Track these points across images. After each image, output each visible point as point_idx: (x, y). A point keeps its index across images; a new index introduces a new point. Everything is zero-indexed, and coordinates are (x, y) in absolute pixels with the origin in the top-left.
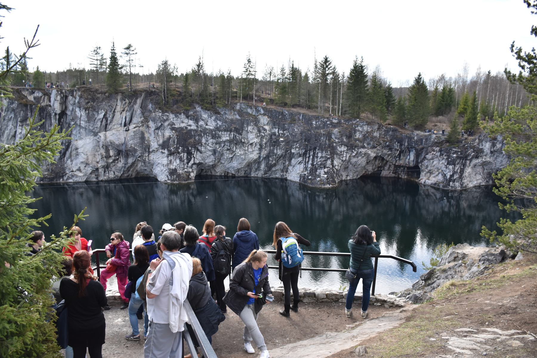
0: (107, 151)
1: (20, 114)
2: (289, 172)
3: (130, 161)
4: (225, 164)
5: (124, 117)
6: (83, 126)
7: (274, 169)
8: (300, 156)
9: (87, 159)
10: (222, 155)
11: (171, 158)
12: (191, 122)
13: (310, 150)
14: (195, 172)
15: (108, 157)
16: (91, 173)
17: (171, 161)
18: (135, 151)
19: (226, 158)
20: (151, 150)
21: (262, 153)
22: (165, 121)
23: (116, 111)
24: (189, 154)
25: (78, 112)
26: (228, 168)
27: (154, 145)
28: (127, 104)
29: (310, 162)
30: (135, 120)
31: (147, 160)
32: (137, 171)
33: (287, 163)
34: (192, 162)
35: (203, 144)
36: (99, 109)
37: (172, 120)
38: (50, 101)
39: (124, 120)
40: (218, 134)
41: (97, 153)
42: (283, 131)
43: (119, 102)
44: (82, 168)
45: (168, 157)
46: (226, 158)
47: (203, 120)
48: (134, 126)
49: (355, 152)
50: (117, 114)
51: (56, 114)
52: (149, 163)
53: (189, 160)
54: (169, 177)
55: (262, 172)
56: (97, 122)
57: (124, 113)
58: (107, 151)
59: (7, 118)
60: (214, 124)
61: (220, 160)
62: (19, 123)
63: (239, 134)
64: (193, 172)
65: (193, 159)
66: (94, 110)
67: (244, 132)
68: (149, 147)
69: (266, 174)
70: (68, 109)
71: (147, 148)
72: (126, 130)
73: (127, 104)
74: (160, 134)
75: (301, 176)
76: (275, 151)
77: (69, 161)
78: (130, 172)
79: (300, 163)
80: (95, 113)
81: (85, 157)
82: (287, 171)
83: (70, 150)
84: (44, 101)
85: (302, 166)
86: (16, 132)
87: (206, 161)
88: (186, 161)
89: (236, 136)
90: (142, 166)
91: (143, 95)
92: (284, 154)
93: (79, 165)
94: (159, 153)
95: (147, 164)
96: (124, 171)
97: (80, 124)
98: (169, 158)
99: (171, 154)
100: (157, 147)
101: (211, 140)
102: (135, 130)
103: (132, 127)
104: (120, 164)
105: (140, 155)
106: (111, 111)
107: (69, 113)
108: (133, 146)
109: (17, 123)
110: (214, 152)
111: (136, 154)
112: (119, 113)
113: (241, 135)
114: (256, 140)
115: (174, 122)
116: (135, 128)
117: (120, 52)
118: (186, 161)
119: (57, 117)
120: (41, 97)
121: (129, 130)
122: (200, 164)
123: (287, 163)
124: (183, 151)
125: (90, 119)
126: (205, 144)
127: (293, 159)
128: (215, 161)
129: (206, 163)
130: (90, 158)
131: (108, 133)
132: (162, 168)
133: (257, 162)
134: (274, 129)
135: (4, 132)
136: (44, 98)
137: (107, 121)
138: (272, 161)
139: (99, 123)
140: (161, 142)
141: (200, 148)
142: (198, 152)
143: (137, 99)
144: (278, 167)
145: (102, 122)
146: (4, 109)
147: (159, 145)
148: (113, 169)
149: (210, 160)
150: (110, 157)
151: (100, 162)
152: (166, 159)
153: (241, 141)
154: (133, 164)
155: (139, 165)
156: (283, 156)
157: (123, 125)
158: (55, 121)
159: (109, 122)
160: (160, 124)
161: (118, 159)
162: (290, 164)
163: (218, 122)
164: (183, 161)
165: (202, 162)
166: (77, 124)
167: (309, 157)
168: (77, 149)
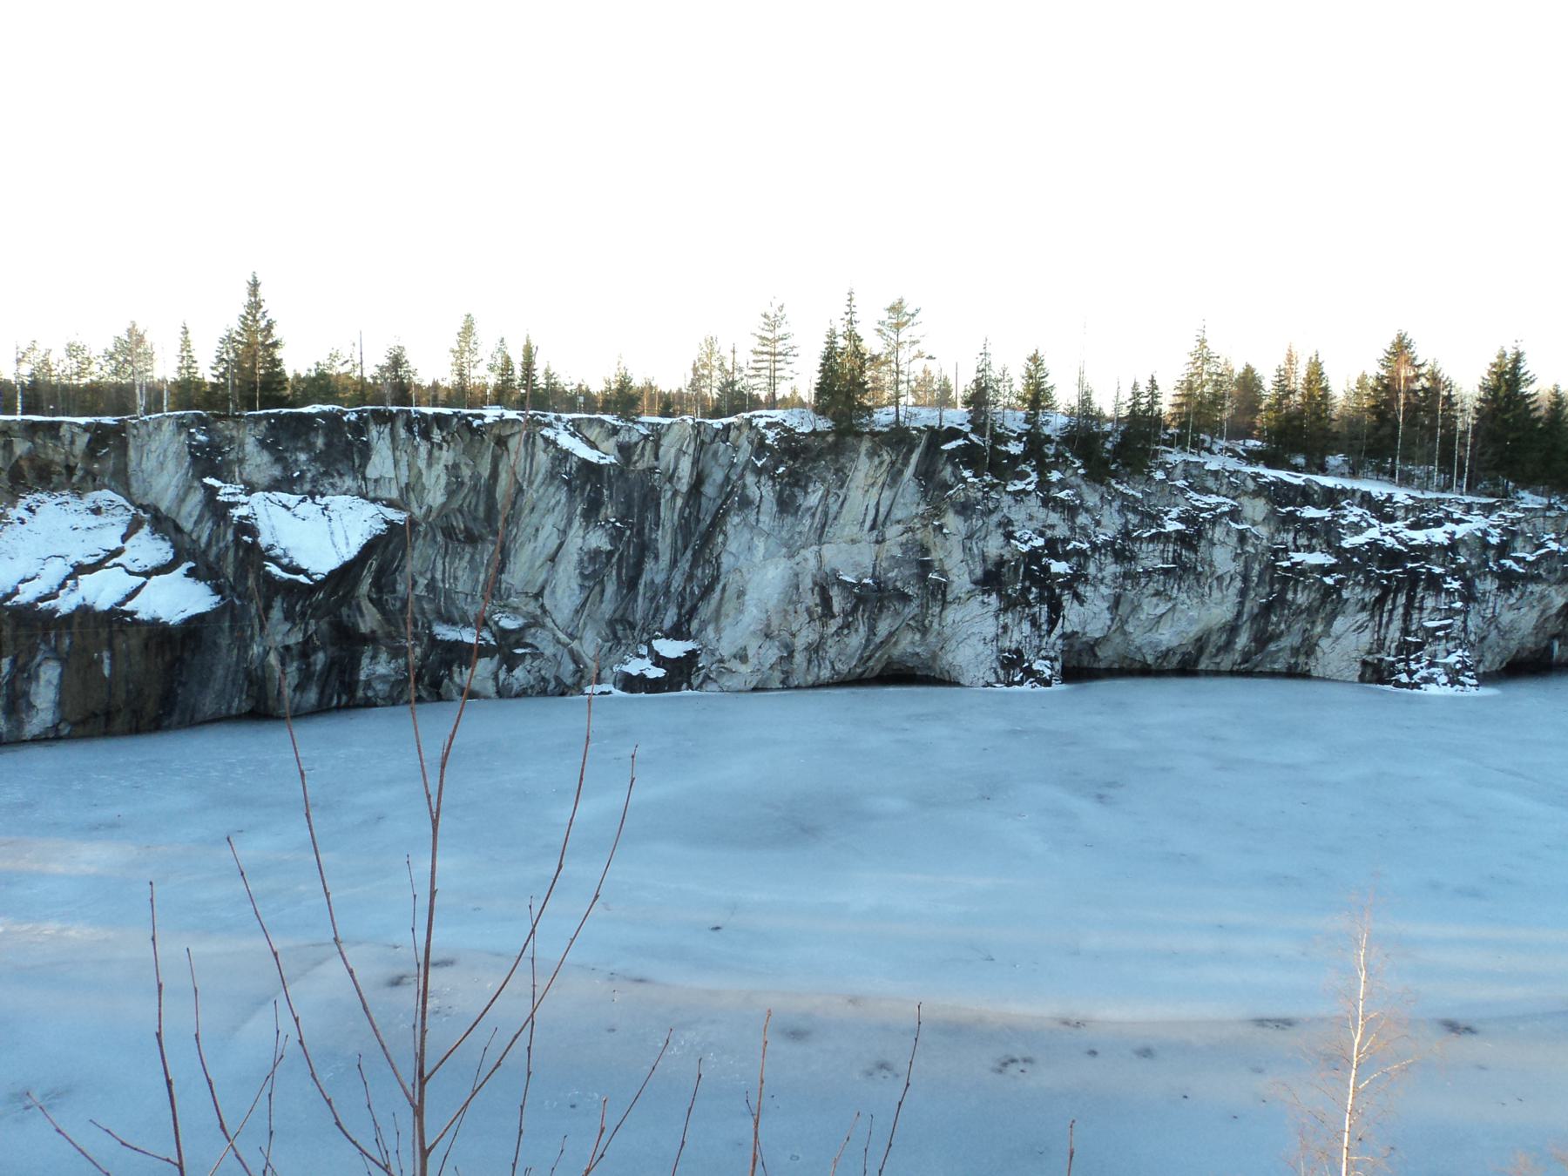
2: (1319, 654)
5: (873, 503)
7: (1272, 647)
8: (1363, 608)
9: (768, 626)
10: (1136, 608)
11: (1008, 618)
12: (1054, 518)
13: (1397, 591)
15: (828, 613)
17: (1005, 628)
18: (905, 598)
19: (1143, 617)
20: (949, 598)
21: (1248, 605)
22: (991, 512)
24: (1056, 609)
25: (753, 492)
26: (1139, 649)
27: (961, 580)
28: (884, 466)
29: (1397, 624)
30: (898, 514)
31: (936, 626)
34: (1057, 631)
38: (657, 458)
39: (872, 513)
40: (1132, 552)
41: (791, 608)
43: (863, 457)
44: (750, 653)
45: (997, 617)
47: (1087, 510)
48: (900, 527)
49: (1517, 594)
51: (675, 493)
53: (1052, 623)
54: (1001, 672)
55: (1237, 657)
57: (875, 491)
58: (826, 601)
59: (542, 505)
61: (1124, 622)
62: (577, 522)
63: (1188, 549)
66: (796, 484)
67: (1203, 543)
71: (938, 593)
72: (877, 542)
73: (884, 466)
75: (1364, 663)
76: (1290, 596)
77: (710, 630)
78: (871, 663)
81: (764, 616)
83: (716, 595)
84: (642, 455)
85: (1366, 638)
86: (560, 546)
88: (1045, 627)
90: (912, 643)
92: (1316, 604)
93: (741, 643)
94: (974, 606)
97: (758, 520)
99: (1008, 605)
104: (856, 640)
105: (917, 611)
107: (709, 490)
108: (899, 584)
112: (861, 491)
113: (1196, 552)
115: (1012, 517)
118: (1045, 627)
119: (679, 502)
120: (637, 444)
121: (884, 540)
123: (1319, 629)
124: (1041, 599)
125: (786, 505)
127: (1340, 618)
130: (775, 622)
131: (828, 551)
132: (981, 647)
133: (1232, 629)
134: (1283, 535)
135: (522, 545)
137: (826, 514)
140: (979, 572)
141: (1081, 589)
145: (813, 515)
147: (975, 583)
148: (832, 653)
150: (833, 616)
151: (804, 632)
152: (991, 621)
154: (891, 634)
156: (1311, 611)
158: (669, 514)
159: (831, 516)
163: (1130, 516)
167: (1391, 612)
168: (741, 594)
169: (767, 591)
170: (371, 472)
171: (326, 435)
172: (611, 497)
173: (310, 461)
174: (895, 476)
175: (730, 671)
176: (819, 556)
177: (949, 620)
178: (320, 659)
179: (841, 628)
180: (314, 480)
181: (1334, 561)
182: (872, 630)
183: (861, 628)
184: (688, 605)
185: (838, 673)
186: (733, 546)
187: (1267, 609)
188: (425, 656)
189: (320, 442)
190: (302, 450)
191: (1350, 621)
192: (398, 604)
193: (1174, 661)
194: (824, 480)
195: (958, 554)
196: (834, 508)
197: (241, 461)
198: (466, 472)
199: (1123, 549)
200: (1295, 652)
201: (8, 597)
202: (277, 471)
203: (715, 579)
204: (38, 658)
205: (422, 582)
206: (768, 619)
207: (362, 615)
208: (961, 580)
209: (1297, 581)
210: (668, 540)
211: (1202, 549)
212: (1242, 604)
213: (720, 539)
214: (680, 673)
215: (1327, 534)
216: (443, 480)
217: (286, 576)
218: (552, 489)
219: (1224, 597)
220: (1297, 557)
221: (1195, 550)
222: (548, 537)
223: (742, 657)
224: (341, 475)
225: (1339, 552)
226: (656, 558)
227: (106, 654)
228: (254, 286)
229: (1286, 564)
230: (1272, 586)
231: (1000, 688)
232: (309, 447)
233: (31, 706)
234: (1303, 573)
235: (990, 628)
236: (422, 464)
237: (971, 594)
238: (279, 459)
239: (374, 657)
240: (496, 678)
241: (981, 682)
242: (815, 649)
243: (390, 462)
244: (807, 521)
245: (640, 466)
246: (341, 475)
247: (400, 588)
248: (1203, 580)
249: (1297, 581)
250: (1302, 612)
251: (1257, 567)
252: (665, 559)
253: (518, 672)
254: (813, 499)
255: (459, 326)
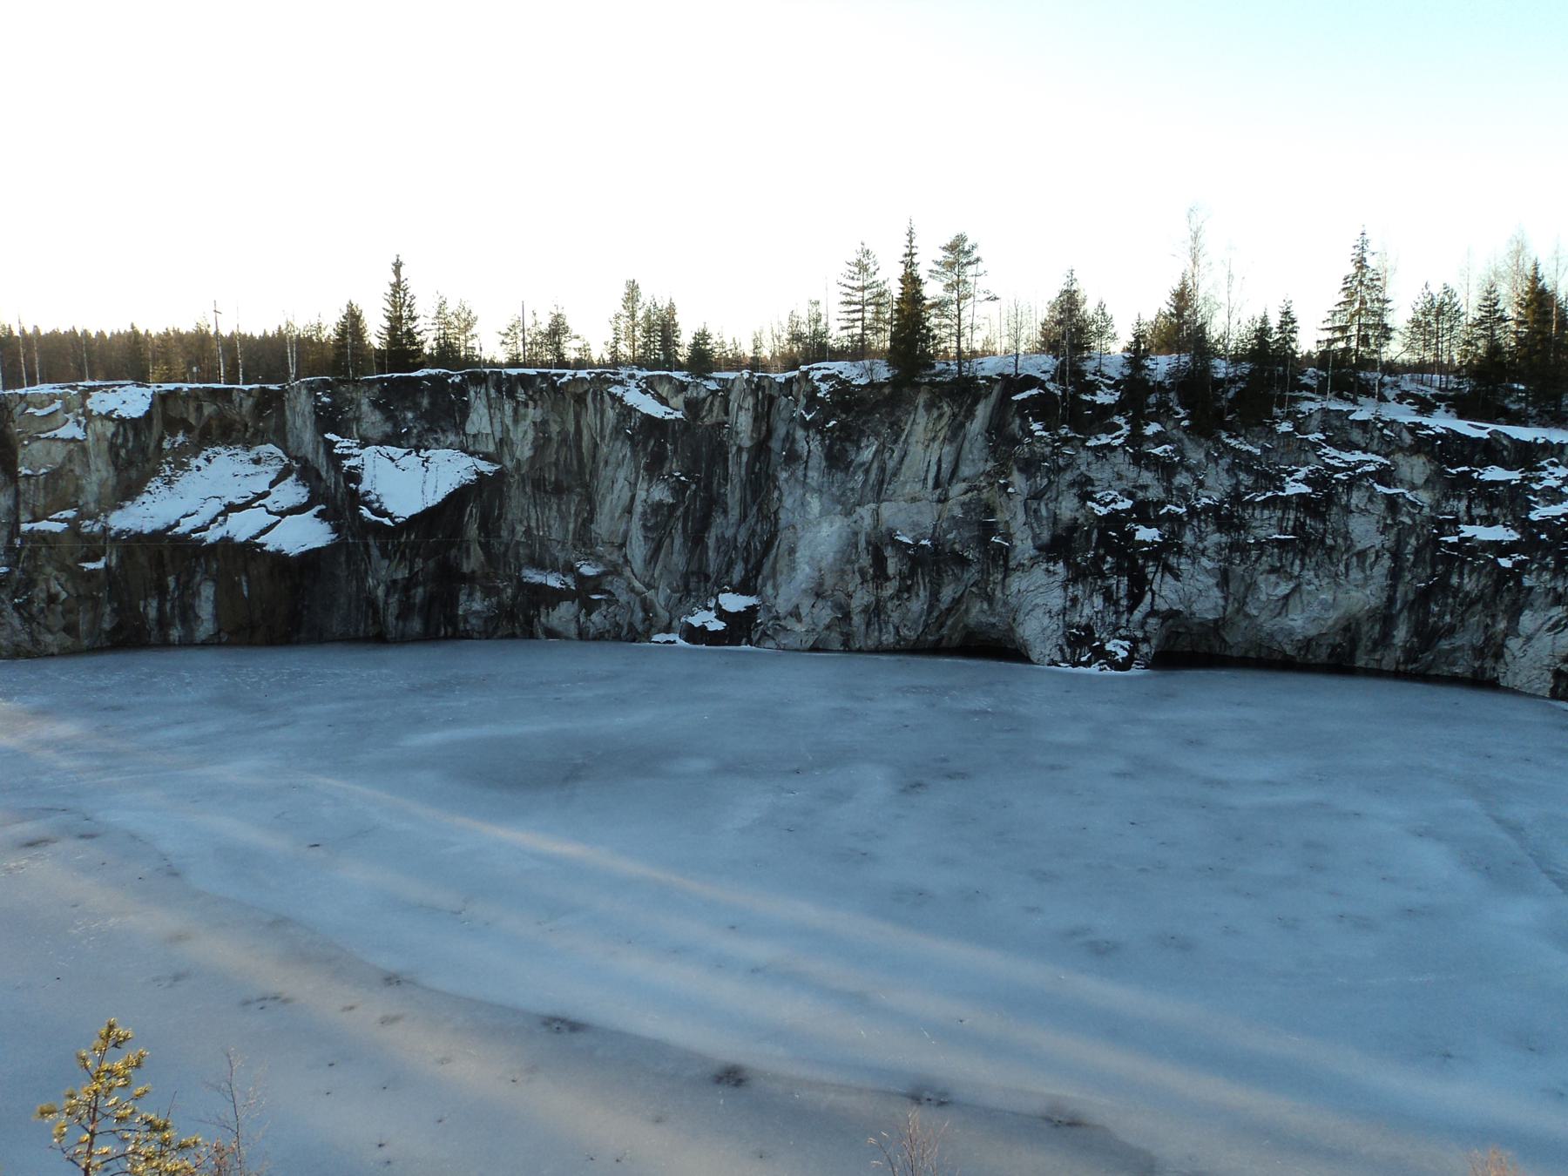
0: (879, 561)
1: (645, 449)
2: (1508, 658)
3: (947, 593)
4: (1262, 619)
5: (934, 460)
6: (814, 484)
7: (1444, 645)
9: (821, 585)
10: (1252, 587)
12: (1147, 477)
14: (1154, 642)
16: (828, 627)
17: (1074, 600)
18: (964, 562)
19: (1263, 597)
20: (1012, 564)
21: (1401, 589)
22: (1060, 470)
23: (912, 440)
25: (802, 447)
27: (1024, 546)
28: (945, 420)
30: (966, 471)
31: (998, 594)
32: (966, 626)
33: (1502, 625)
34: (1144, 607)
35: (1186, 548)
36: (862, 433)
37: (1083, 468)
38: (727, 414)
39: (934, 469)
40: (1241, 518)
42: (1489, 509)
43: (921, 411)
44: (804, 611)
45: (1066, 589)
46: (1263, 597)
47: (1188, 469)
48: (964, 485)
50: (916, 450)
51: (740, 449)
52: (1005, 603)
53: (1135, 599)
54: (1067, 650)
56: (855, 473)
57: (936, 445)
58: (879, 561)
59: (612, 460)
60: (1227, 482)
61: (1243, 603)
64: (1146, 640)
65: (1148, 596)
66: (848, 438)
68: (1004, 554)
69: (1415, 661)
70: (775, 436)
71: (1000, 559)
72: (939, 501)
73: (945, 420)
74: (1044, 512)
76: (1455, 580)
77: (769, 584)
78: (945, 631)
79: (1555, 626)
80: (848, 445)
82: (1498, 656)
84: (711, 410)
86: (633, 498)
87: (1195, 607)
89: (1303, 524)
91: (995, 393)
93: (795, 600)
94: (1038, 575)
95: (999, 608)
96: (926, 625)
97: (805, 476)
98: (1071, 589)
99: (1077, 575)
100: (1033, 552)
101: (1216, 537)
102: (966, 498)
103: (957, 489)
104: (917, 605)
105: (977, 576)
106: (895, 442)
107: (775, 445)
108: (957, 547)
109: (637, 473)
110: (1224, 579)
111: (966, 576)
112: (920, 447)
114: (1378, 540)
115: (1092, 475)
116: (966, 493)
117: (928, 260)
118: (1124, 602)
119: (745, 457)
120: (705, 400)
122: (1172, 614)
123: (1502, 625)
124: (1118, 570)
126: (1193, 548)
128: (1225, 609)
129: (1193, 614)
130: (829, 581)
131: (887, 510)
132: (1046, 621)
133: (1385, 617)
135: (604, 496)
136: (712, 403)
137: (882, 469)
138: (1441, 615)
139: (860, 477)
140: (1046, 536)
141: (1173, 560)
142: (1168, 578)
143: (976, 402)
144: (1461, 639)
145: (867, 472)
146: (608, 432)
147: (1039, 548)
148: (895, 617)
149: (1208, 605)
150: (888, 579)
151: (859, 594)
152: (1059, 592)
153: (1322, 541)
154: (957, 602)
155: (974, 611)
157: (930, 482)
159: (888, 473)
160: (1045, 481)
161: (909, 589)
162: (1512, 630)
163: (1242, 476)
164: (1117, 603)
165: (1181, 608)
166: (797, 480)
169: (822, 549)
170: (471, 429)
171: (431, 396)
172: (675, 452)
173: (416, 419)
174: (956, 431)
175: (784, 629)
176: (876, 513)
177: (1014, 588)
178: (419, 593)
179: (900, 591)
180: (419, 436)
181: (1516, 536)
182: (934, 596)
183: (922, 593)
184: (753, 560)
185: (905, 639)
186: (788, 502)
187: (1425, 596)
188: (515, 597)
189: (425, 402)
190: (409, 409)
191: (1541, 617)
192: (502, 549)
193: (1323, 654)
194: (877, 435)
195: (1021, 517)
196: (891, 464)
197: (358, 420)
198: (554, 428)
199: (1231, 515)
200: (1479, 653)
201: (170, 528)
202: (388, 428)
203: (774, 535)
204: (198, 578)
205: (520, 529)
206: (821, 577)
207: (468, 557)
208: (1024, 546)
209: (1464, 562)
210: (738, 495)
211: (1334, 518)
212: (1393, 587)
213: (776, 494)
214: (739, 628)
215: (1510, 502)
216: (531, 435)
217: (374, 518)
218: (619, 444)
219: (1366, 579)
220: (1468, 531)
221: (1322, 518)
222: (621, 492)
223: (795, 614)
224: (444, 431)
225: (1524, 525)
226: (725, 512)
227: (244, 578)
228: (397, 267)
229: (1453, 539)
230: (1434, 568)
231: (1065, 668)
232: (415, 407)
233: (197, 617)
234: (1472, 551)
235: (1056, 600)
236: (508, 421)
237: (1034, 561)
238: (390, 417)
239: (470, 595)
240: (578, 621)
241: (1047, 660)
242: (875, 612)
243: (486, 419)
244: (860, 477)
245: (707, 421)
246: (444, 431)
247: (504, 533)
248: (1335, 556)
249: (1464, 562)
250: (1473, 603)
251: (1413, 541)
252: (734, 514)
253: (595, 617)
254: (867, 455)
255: (622, 291)
